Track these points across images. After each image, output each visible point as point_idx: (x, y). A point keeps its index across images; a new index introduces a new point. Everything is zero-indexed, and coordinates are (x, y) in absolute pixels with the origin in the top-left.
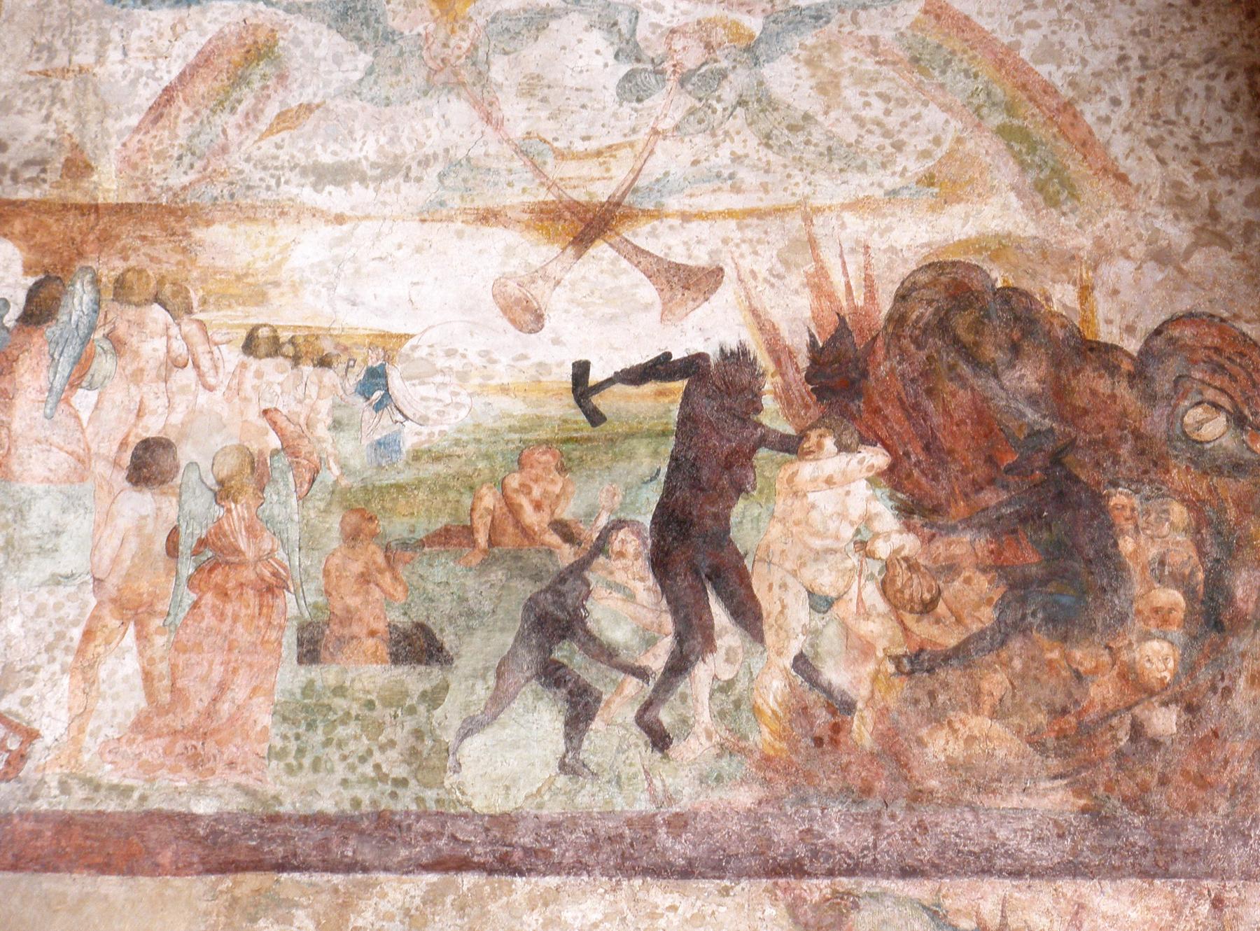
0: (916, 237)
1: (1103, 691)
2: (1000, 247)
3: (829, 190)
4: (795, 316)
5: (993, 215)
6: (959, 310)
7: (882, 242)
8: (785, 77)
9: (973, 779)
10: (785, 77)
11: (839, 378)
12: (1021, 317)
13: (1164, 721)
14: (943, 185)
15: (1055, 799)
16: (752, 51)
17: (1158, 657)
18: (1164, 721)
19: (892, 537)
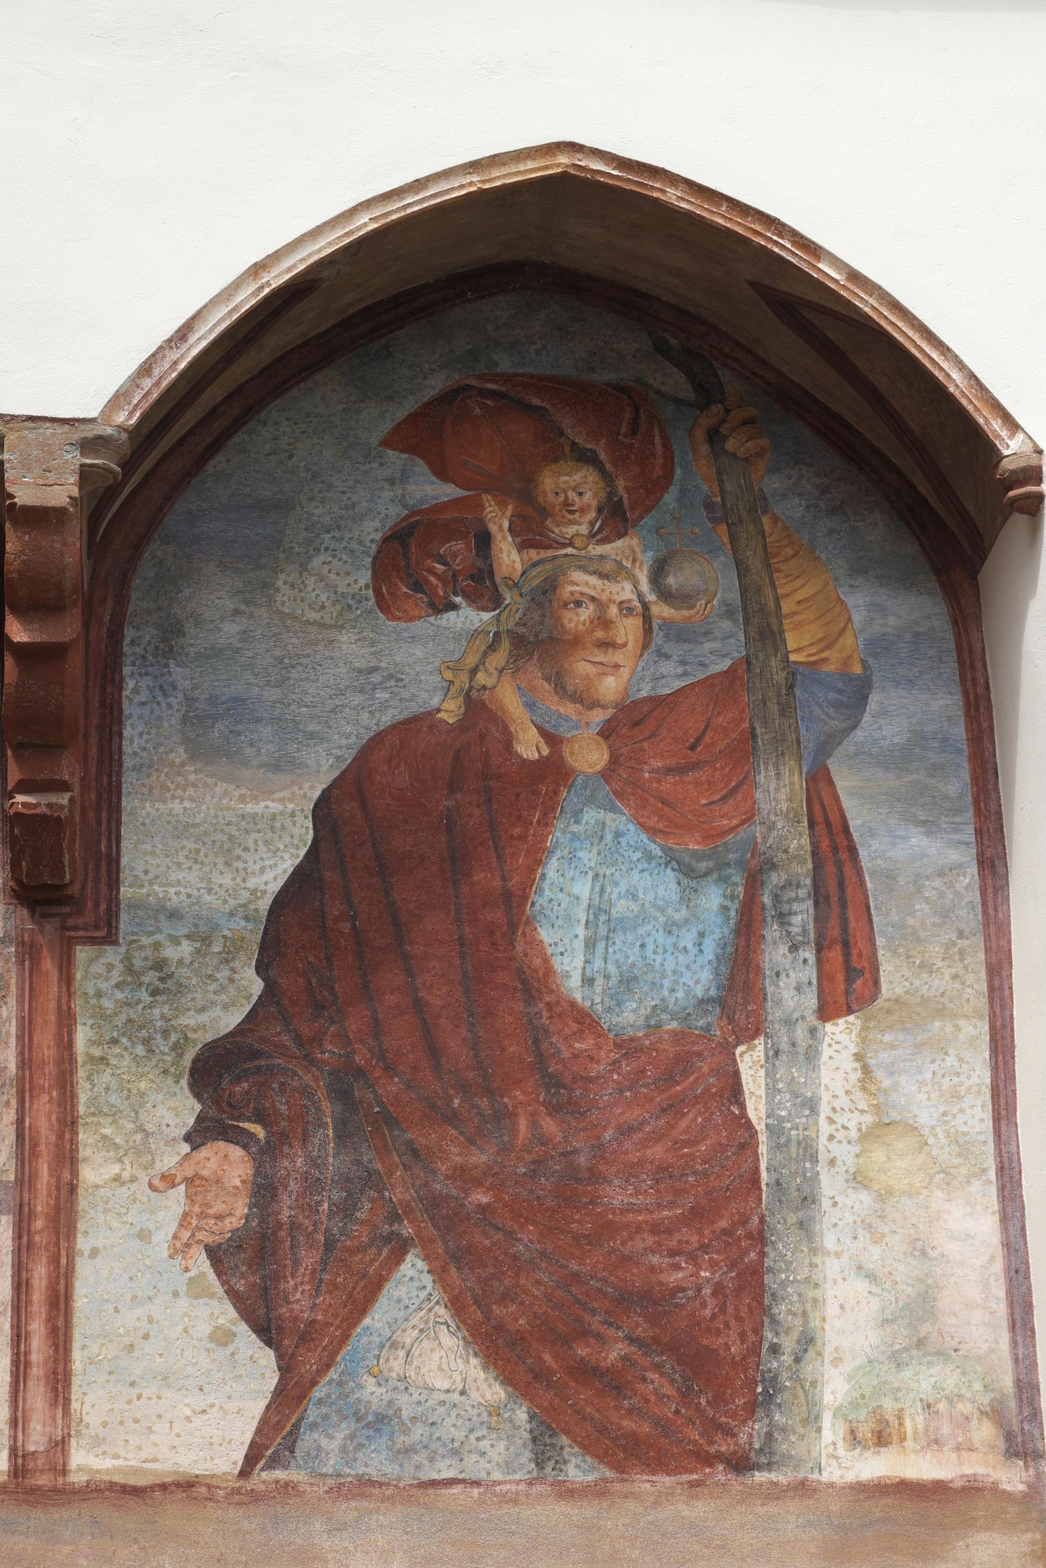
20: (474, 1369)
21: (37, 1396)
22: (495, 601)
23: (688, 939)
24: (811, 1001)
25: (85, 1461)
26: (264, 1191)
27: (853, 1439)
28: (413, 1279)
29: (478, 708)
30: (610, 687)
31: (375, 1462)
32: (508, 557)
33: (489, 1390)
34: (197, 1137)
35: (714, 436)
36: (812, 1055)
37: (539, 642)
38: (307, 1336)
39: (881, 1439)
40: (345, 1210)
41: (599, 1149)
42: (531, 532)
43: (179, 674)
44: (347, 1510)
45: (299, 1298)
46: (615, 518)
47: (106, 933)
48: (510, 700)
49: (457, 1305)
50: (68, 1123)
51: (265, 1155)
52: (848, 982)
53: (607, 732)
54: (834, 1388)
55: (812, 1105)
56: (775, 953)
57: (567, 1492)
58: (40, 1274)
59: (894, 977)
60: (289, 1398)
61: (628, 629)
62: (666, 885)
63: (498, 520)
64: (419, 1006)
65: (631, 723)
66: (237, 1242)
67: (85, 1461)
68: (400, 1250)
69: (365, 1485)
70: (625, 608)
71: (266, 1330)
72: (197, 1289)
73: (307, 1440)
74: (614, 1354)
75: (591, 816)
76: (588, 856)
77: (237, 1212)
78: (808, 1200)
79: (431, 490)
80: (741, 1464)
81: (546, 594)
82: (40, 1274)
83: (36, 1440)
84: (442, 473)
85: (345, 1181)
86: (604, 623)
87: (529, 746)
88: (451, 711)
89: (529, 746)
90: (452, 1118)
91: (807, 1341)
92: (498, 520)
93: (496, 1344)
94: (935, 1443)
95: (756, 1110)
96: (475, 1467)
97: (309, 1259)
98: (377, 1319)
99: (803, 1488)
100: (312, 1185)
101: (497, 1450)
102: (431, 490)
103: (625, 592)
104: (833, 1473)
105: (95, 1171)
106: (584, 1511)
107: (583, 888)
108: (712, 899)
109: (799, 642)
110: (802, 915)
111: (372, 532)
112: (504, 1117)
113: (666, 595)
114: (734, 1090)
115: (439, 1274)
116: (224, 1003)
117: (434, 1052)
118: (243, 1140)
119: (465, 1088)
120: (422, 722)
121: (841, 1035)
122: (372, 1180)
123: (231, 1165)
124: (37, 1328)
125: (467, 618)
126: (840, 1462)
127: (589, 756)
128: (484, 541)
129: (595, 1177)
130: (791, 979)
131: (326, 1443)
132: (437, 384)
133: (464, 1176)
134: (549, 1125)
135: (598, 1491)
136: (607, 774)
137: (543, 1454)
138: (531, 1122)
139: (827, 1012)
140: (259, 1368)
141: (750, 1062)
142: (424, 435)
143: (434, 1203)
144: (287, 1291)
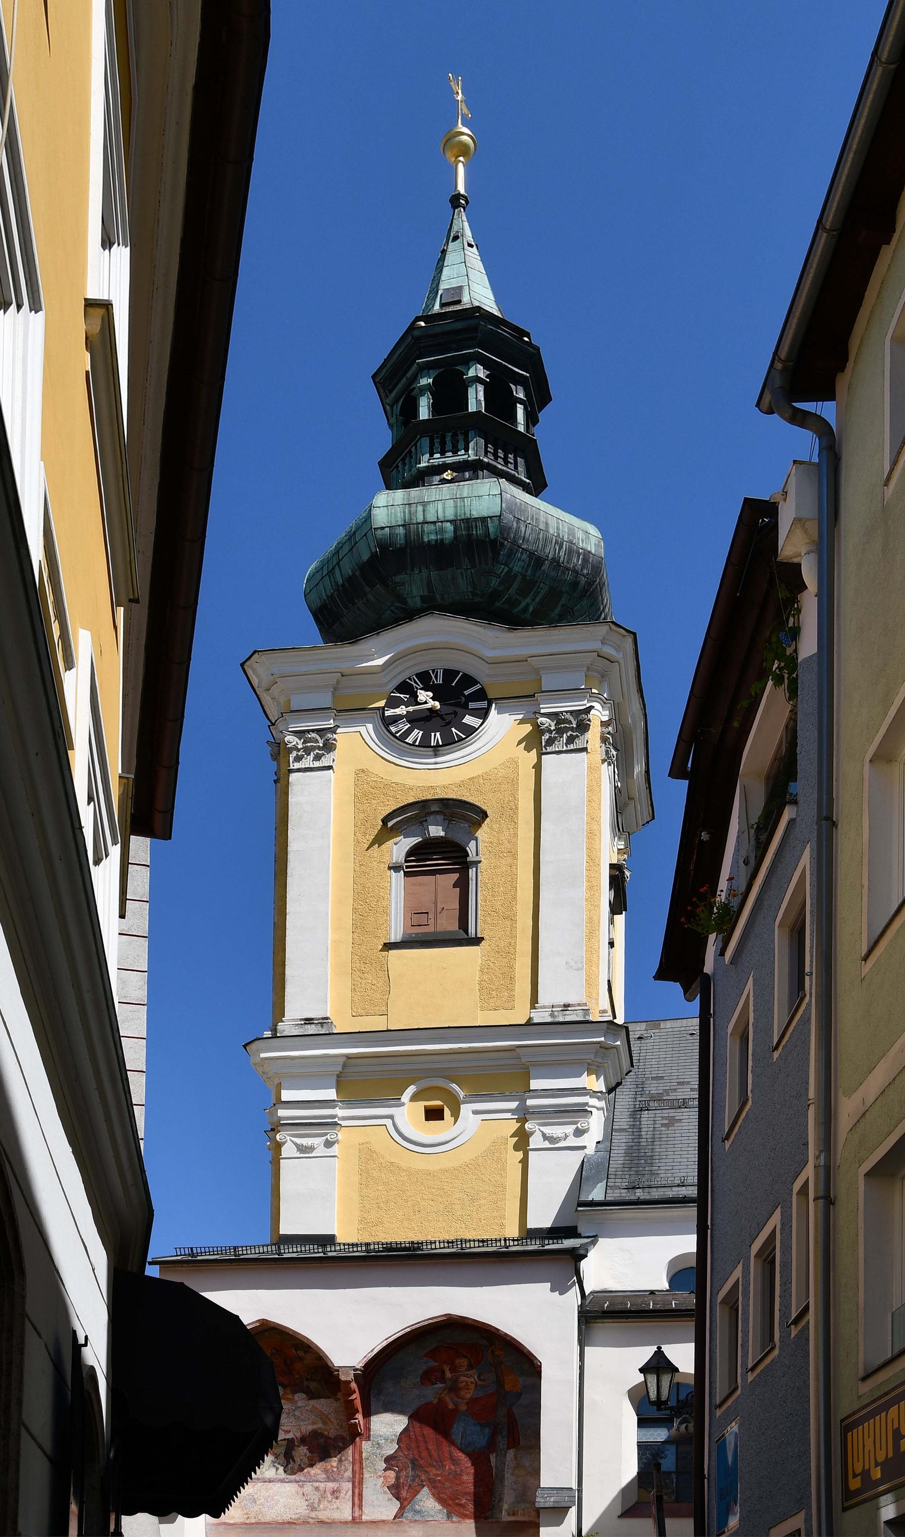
0: (310, 1428)
1: (329, 1467)
2: (320, 1428)
3: (302, 1423)
4: (298, 1435)
5: (320, 1425)
6: (315, 1434)
7: (308, 1428)
8: (297, 1413)
9: (316, 1474)
10: (297, 1413)
11: (303, 1440)
12: (322, 1435)
13: (335, 1469)
14: (313, 1423)
15: (324, 1476)
16: (294, 1411)
17: (335, 1464)
18: (335, 1469)
19: (308, 1454)
20: (437, 1504)
21: (356, 1508)
22: (445, 1382)
23: (482, 1437)
24: (506, 1446)
25: (364, 1518)
26: (398, 1478)
27: (508, 1514)
28: (426, 1490)
29: (441, 1401)
30: (468, 1396)
31: (417, 1518)
32: (448, 1375)
33: (438, 1507)
34: (385, 1470)
35: (493, 1352)
36: (505, 1456)
37: (454, 1388)
38: (405, 1499)
39: (514, 1515)
40: (413, 1480)
41: (462, 1471)
42: (453, 1370)
43: (382, 1398)
44: (412, 1525)
45: (404, 1494)
46: (470, 1367)
47: (368, 1438)
48: (448, 1399)
49: (433, 1495)
50: (361, 1468)
51: (398, 1473)
52: (514, 1443)
53: (467, 1403)
54: (505, 1507)
55: (505, 1464)
56: (499, 1438)
57: (453, 1522)
58: (357, 1491)
59: (522, 1443)
60: (402, 1508)
61: (472, 1386)
62: (478, 1428)
63: (447, 1369)
64: (428, 1449)
65: (472, 1402)
66: (393, 1486)
67: (364, 1518)
68: (424, 1486)
69: (416, 1521)
70: (472, 1383)
71: (398, 1499)
72: (385, 1493)
73: (405, 1515)
74: (464, 1501)
75: (463, 1417)
76: (462, 1425)
77: (393, 1481)
78: (503, 1478)
79: (432, 1364)
80: (486, 1518)
81: (455, 1381)
82: (357, 1491)
83: (357, 1514)
84: (435, 1361)
85: (413, 1476)
86: (467, 1385)
87: (451, 1406)
88: (435, 1401)
89: (451, 1406)
90: (434, 1466)
91: (501, 1500)
92: (447, 1369)
93: (440, 1500)
94: (524, 1515)
95: (493, 1464)
96: (436, 1518)
97: (406, 1488)
98: (418, 1497)
99: (498, 1522)
100: (407, 1477)
101: (440, 1516)
102: (432, 1364)
103: (472, 1380)
104: (504, 1519)
105: (366, 1475)
106: (457, 1525)
107: (461, 1430)
108: (487, 1431)
109: (507, 1387)
110: (505, 1433)
111: (420, 1372)
112: (444, 1466)
113: (480, 1380)
114: (489, 1461)
115: (430, 1490)
116: (391, 1449)
117: (430, 1456)
118: (394, 1470)
119: (436, 1461)
120: (431, 1403)
121: (511, 1453)
122: (418, 1476)
123: (392, 1474)
124: (356, 1498)
125: (439, 1385)
126: (505, 1517)
127: (463, 1408)
128: (443, 1372)
129: (461, 1475)
130: (502, 1443)
131: (409, 1515)
132: (434, 1346)
133: (437, 1475)
134: (452, 1467)
135: (459, 1522)
136: (467, 1410)
137: (449, 1516)
138: (449, 1466)
139: (509, 1448)
140: (397, 1504)
141: (493, 1458)
142: (431, 1354)
143: (429, 1479)
144: (402, 1492)
